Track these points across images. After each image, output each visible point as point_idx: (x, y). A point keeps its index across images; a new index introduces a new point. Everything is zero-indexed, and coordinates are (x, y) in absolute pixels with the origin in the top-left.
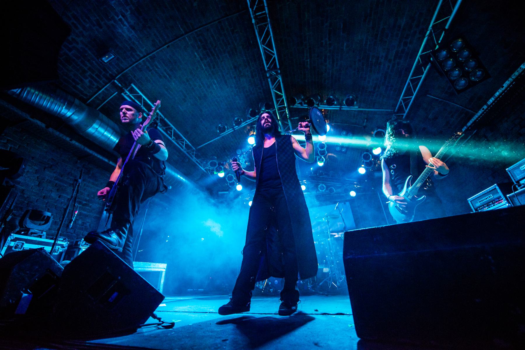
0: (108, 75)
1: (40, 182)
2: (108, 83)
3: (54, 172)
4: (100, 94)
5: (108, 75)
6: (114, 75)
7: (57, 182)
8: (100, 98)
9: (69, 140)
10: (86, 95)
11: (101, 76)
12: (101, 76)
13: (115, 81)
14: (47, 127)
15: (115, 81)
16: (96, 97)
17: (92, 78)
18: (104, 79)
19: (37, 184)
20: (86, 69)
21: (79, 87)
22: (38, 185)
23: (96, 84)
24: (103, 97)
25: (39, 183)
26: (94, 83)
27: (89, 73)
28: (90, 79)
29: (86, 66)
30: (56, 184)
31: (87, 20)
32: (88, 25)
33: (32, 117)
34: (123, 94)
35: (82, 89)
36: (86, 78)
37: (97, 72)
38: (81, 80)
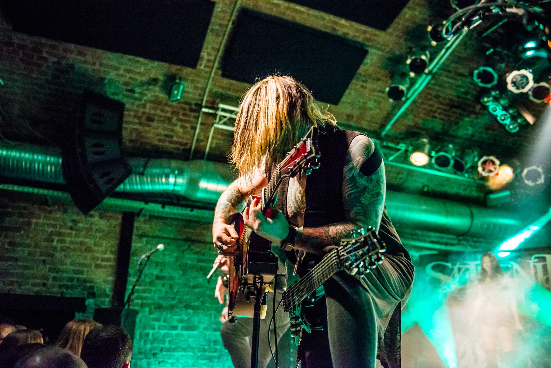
0: (193, 107)
4: (199, 134)
5: (193, 107)
6: (199, 102)
7: (200, 264)
8: (202, 138)
10: (186, 144)
12: (187, 112)
13: (204, 110)
15: (204, 110)
18: (193, 114)
20: (169, 115)
21: (175, 139)
23: (188, 125)
24: (204, 136)
27: (175, 118)
28: (179, 124)
29: (167, 112)
31: (138, 65)
36: (175, 125)
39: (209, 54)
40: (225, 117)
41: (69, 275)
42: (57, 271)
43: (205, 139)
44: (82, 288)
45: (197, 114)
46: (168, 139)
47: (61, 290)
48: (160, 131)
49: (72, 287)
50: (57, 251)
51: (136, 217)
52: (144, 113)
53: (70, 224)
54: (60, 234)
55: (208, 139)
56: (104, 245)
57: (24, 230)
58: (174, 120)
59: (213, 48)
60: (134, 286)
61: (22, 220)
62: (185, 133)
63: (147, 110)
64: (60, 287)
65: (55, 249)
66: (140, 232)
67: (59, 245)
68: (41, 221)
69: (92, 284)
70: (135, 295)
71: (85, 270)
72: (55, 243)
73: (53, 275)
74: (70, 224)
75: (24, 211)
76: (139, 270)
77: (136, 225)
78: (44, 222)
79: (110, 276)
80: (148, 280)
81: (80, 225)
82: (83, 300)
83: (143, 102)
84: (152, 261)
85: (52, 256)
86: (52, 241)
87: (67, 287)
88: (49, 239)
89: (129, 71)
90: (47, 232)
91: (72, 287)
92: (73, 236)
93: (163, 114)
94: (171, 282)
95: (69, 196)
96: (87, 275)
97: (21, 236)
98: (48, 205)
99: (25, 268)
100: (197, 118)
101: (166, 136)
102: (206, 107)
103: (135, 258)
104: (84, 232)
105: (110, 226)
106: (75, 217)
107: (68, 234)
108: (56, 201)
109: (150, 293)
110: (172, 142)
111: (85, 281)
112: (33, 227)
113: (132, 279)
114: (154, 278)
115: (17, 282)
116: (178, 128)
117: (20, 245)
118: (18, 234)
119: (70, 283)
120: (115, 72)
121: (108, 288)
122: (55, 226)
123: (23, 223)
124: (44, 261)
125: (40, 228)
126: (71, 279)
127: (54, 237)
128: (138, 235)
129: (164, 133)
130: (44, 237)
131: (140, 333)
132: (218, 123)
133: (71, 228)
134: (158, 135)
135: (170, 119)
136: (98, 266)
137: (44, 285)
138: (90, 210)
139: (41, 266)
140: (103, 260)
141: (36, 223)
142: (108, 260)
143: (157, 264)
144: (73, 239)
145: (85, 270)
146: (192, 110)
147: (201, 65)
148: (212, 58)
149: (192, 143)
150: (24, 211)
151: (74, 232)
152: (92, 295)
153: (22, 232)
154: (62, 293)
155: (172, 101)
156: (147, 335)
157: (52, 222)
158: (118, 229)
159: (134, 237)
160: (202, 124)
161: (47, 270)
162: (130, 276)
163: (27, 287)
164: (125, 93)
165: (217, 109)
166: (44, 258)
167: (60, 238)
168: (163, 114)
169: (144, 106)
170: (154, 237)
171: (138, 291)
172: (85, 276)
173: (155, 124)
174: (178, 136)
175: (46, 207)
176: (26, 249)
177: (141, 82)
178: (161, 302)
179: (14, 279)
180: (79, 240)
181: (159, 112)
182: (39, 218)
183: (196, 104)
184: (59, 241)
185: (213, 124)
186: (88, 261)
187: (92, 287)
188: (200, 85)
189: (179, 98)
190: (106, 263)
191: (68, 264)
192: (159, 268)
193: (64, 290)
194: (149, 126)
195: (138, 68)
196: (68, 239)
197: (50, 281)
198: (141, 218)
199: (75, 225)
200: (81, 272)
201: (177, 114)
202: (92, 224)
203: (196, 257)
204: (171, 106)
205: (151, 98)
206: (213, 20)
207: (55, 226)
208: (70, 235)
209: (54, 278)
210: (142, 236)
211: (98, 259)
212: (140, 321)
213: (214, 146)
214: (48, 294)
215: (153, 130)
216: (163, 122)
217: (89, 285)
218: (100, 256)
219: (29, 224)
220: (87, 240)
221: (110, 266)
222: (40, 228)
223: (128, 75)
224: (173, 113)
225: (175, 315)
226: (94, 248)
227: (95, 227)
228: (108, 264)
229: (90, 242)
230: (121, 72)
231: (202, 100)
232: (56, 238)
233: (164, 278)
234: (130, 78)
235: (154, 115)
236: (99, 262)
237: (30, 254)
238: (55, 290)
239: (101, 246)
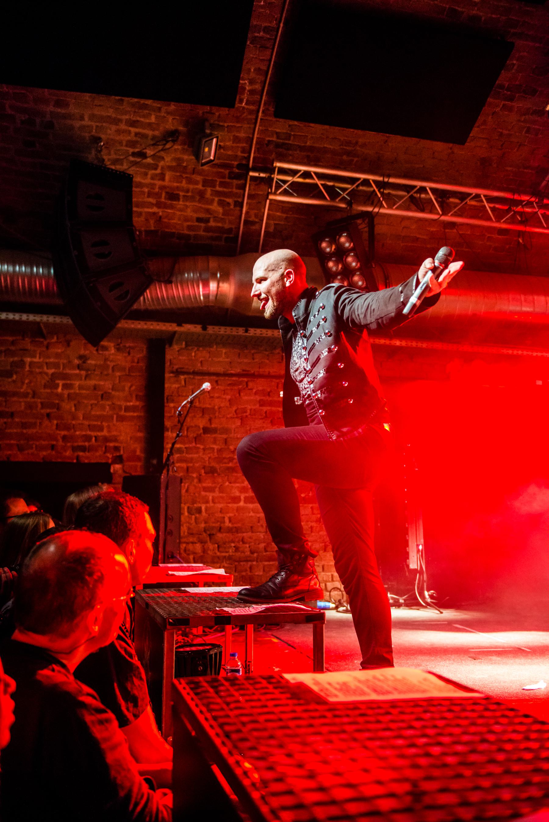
1: (241, 419)
3: (256, 393)
4: (247, 213)
6: (244, 162)
7: (265, 409)
8: (253, 218)
9: (244, 331)
10: (230, 230)
11: (227, 180)
14: (204, 328)
15: (251, 174)
16: (245, 221)
17: (218, 193)
18: (235, 182)
19: (239, 424)
20: (200, 187)
21: (212, 224)
22: (241, 424)
24: (256, 216)
25: (240, 421)
26: (228, 200)
28: (216, 199)
29: (197, 183)
30: (266, 412)
31: (146, 112)
32: (153, 119)
33: (179, 325)
35: (220, 225)
36: (211, 202)
37: (218, 180)
38: (208, 211)
39: (251, 82)
40: (285, 182)
41: (84, 433)
42: (67, 427)
43: (257, 220)
44: (104, 449)
45: (241, 182)
46: (203, 225)
47: (76, 454)
48: (189, 213)
49: (90, 449)
50: (63, 401)
51: (167, 346)
52: (162, 188)
53: (76, 362)
54: (65, 377)
56: (127, 389)
57: (16, 373)
59: (258, 71)
60: (173, 444)
61: (12, 359)
62: (225, 213)
63: (166, 183)
64: (74, 449)
65: (60, 396)
66: (176, 367)
67: (66, 392)
68: (36, 360)
69: (117, 444)
70: (176, 456)
71: (105, 424)
72: (60, 390)
73: (63, 433)
74: (76, 362)
75: (13, 348)
76: (179, 421)
77: (168, 357)
78: (41, 360)
79: (139, 431)
80: (192, 435)
81: (91, 362)
82: (107, 466)
83: (159, 171)
84: (195, 407)
85: (58, 407)
86: (57, 386)
87: (83, 449)
88: (51, 384)
89: (133, 124)
90: (47, 374)
91: (90, 449)
92: (83, 378)
93: (191, 187)
94: (225, 436)
95: (70, 322)
96: (109, 431)
97: (14, 381)
98: (44, 337)
99: (24, 425)
100: (243, 187)
101: (199, 220)
102: (254, 169)
103: (172, 405)
104: (97, 372)
105: (133, 362)
106: (82, 352)
107: (77, 375)
108: (54, 329)
109: (197, 453)
111: (106, 439)
112: (27, 368)
113: (170, 435)
114: (202, 431)
115: (18, 445)
116: (215, 207)
117: (15, 394)
118: (10, 380)
119: (87, 444)
120: (114, 128)
121: (138, 449)
122: (56, 366)
123: (13, 364)
124: (48, 415)
125: (37, 370)
126: (88, 438)
127: (57, 382)
128: (172, 372)
129: (195, 215)
130: (43, 382)
131: (188, 508)
132: (275, 194)
133: (79, 367)
134: (186, 220)
135: (202, 194)
136: (121, 419)
137: (53, 447)
138: (101, 339)
139: (46, 422)
140: (127, 409)
141: (31, 364)
142: (134, 409)
143: (204, 411)
144: (83, 382)
145: (105, 424)
147: (241, 101)
148: (258, 87)
150: (13, 348)
151: (83, 373)
152: (119, 459)
153: (15, 377)
154: (78, 457)
155: (203, 165)
156: (199, 511)
157: (52, 360)
158: (142, 364)
159: (167, 375)
160: (250, 197)
161: (54, 427)
162: (168, 430)
163: (30, 451)
164: (132, 159)
165: (271, 170)
166: (48, 411)
167: (64, 382)
169: (162, 177)
170: (195, 373)
171: (180, 451)
172: (105, 433)
173: (181, 203)
174: (216, 219)
175: (42, 340)
176: (21, 400)
177: (154, 138)
178: (213, 464)
179: (12, 442)
180: (92, 382)
181: (184, 184)
182: (35, 357)
183: (239, 166)
184: (65, 386)
185: (267, 198)
186: (107, 411)
187: (117, 449)
188: (242, 135)
189: (212, 158)
190: (131, 414)
191: (81, 418)
192: (207, 417)
193: (81, 454)
194: (172, 207)
195: (144, 116)
196: (77, 383)
197: (61, 443)
198: (176, 347)
199: (84, 362)
200: (101, 429)
201: (212, 184)
202: (106, 360)
203: (258, 398)
204: (200, 173)
205: (170, 164)
206: (254, 22)
207: (56, 366)
208: (79, 377)
209: (64, 438)
210: (178, 373)
211: (120, 407)
212: (187, 491)
213: (271, 229)
214: (59, 460)
215: (178, 213)
216: (192, 199)
217: (112, 444)
218: (123, 404)
219: (22, 364)
220: (102, 383)
221: (138, 417)
222: (37, 370)
223: (133, 130)
224: (205, 183)
225: (235, 482)
226: (113, 393)
227: (111, 364)
228: (135, 414)
229: (107, 385)
230: (123, 126)
232: (61, 383)
233: (215, 431)
234: (136, 134)
236: (122, 413)
237: (30, 406)
238: (68, 453)
239: (123, 390)
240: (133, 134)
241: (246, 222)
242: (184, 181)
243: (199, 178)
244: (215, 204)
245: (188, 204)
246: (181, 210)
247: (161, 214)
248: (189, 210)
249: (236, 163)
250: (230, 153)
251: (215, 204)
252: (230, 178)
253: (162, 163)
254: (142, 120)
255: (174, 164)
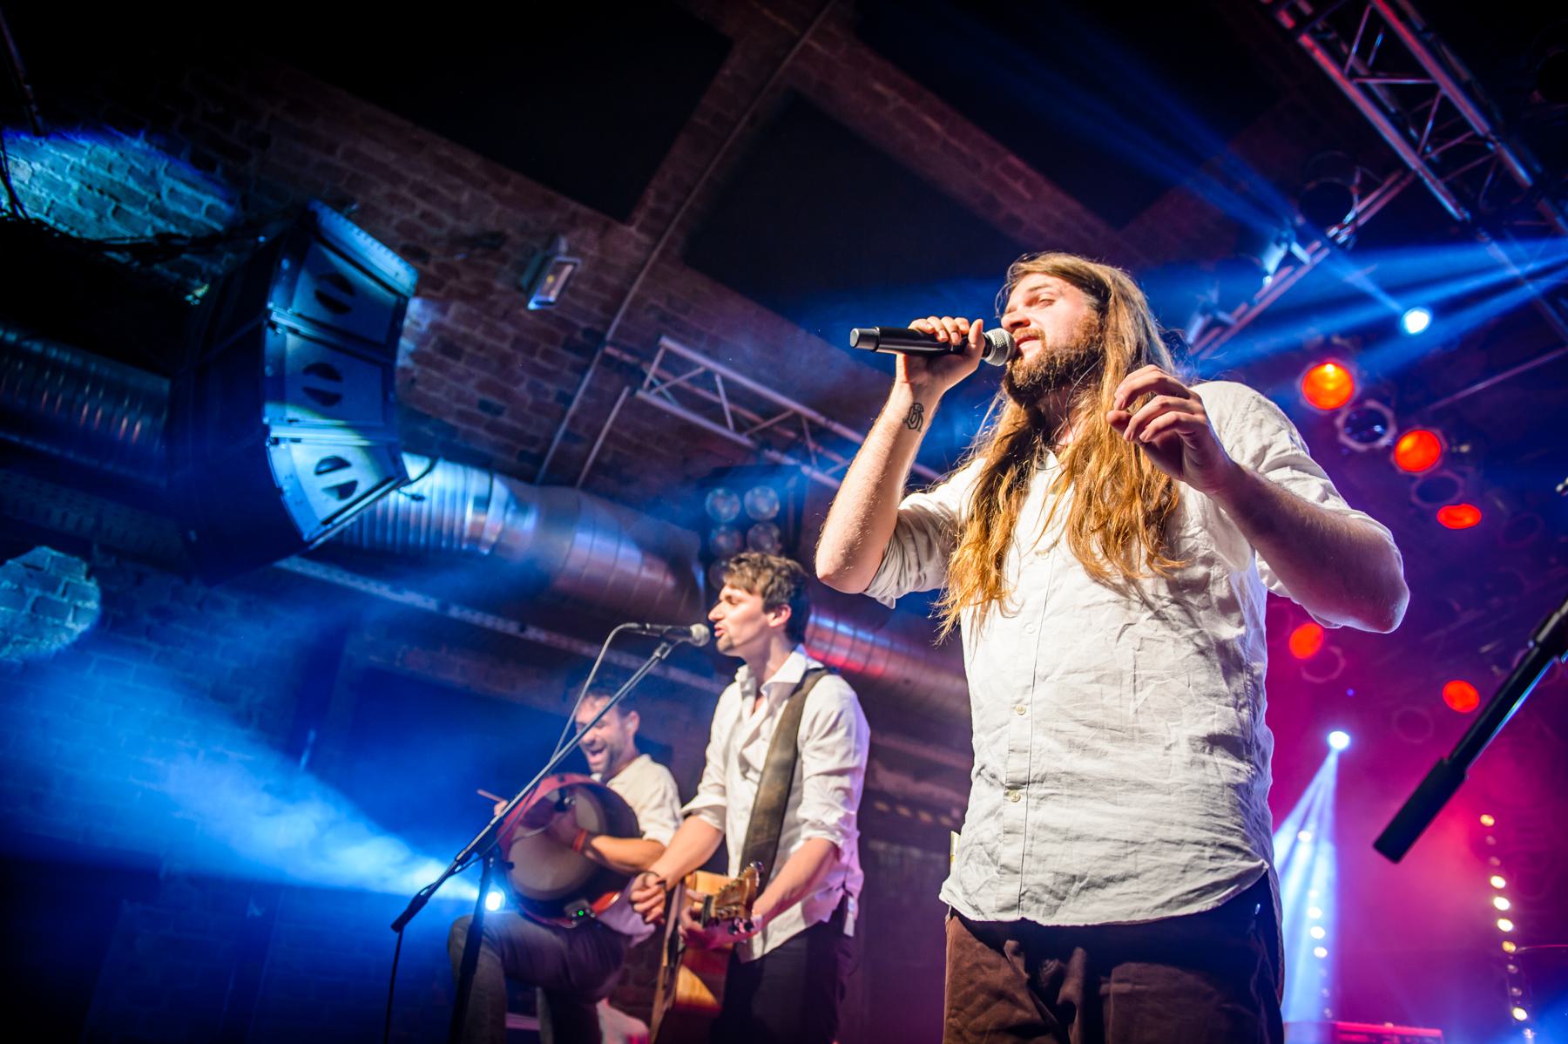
0: (579, 336)
2: (586, 368)
6: (599, 328)
8: (580, 431)
10: (533, 441)
13: (609, 350)
18: (572, 357)
20: (506, 347)
21: (504, 419)
23: (551, 387)
27: (520, 356)
29: (502, 337)
34: (641, 394)
35: (518, 425)
36: (517, 382)
46: (487, 416)
48: (470, 388)
55: (595, 438)
58: (517, 366)
90: (70, 631)
93: (490, 341)
100: (582, 371)
101: (485, 406)
102: (614, 344)
110: (493, 428)
129: (479, 396)
135: (505, 360)
146: (570, 345)
149: (550, 441)
160: (589, 391)
168: (490, 341)
173: (460, 367)
183: (588, 332)
194: (440, 367)
213: (606, 459)
223: (422, 205)
224: (517, 343)
231: (607, 325)
234: (424, 215)
235: (465, 338)
240: (417, 212)
241: (567, 435)
242: (481, 328)
243: (510, 330)
244: (523, 387)
245: (473, 370)
246: (458, 378)
247: (416, 374)
248: (472, 383)
249: (583, 325)
250: (580, 303)
251: (523, 387)
252: (566, 346)
253: (452, 282)
254: (444, 191)
255: (473, 291)
